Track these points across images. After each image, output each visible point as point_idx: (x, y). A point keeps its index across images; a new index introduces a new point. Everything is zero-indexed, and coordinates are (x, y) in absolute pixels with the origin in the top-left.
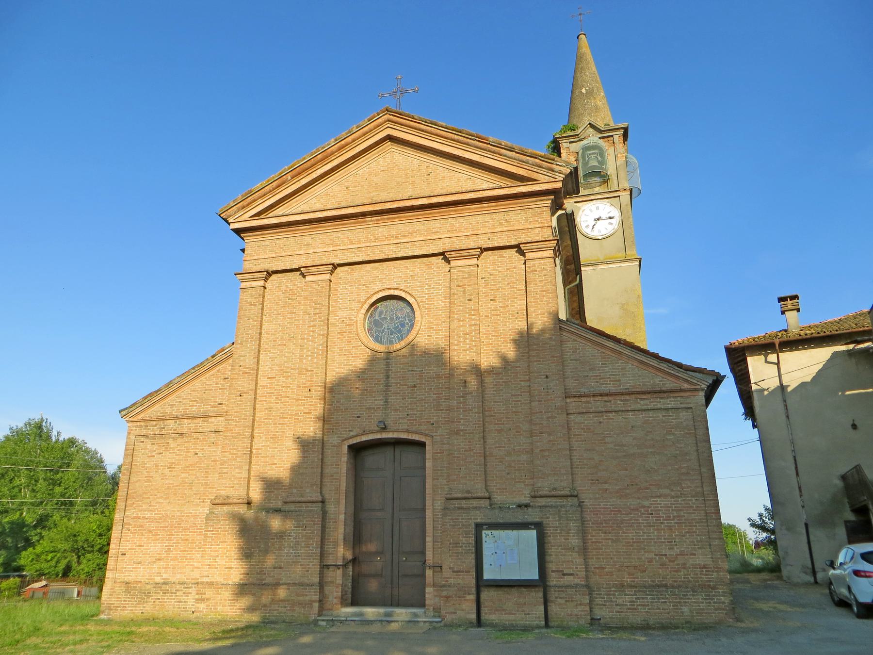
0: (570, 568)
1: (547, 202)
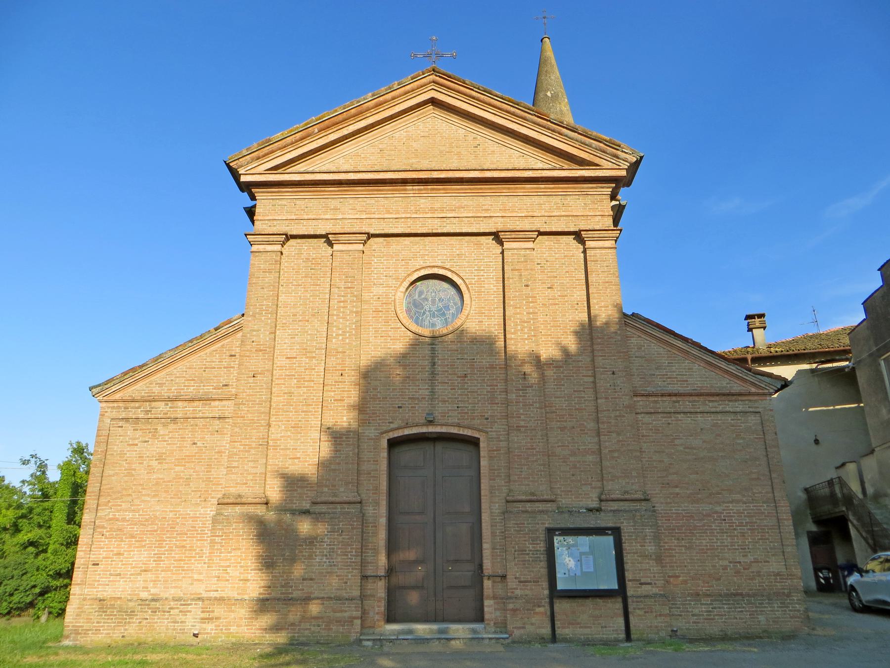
0: (648, 577)
1: (607, 190)
